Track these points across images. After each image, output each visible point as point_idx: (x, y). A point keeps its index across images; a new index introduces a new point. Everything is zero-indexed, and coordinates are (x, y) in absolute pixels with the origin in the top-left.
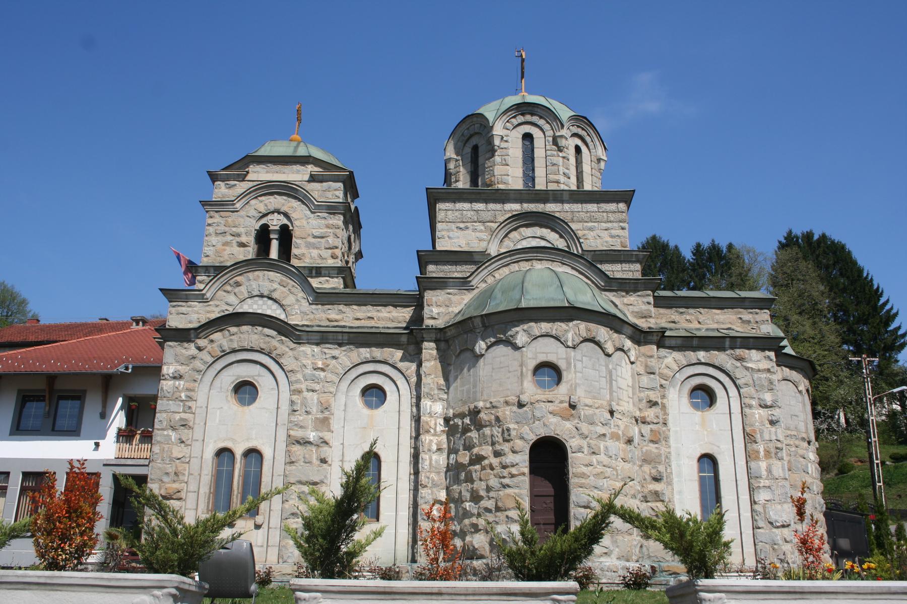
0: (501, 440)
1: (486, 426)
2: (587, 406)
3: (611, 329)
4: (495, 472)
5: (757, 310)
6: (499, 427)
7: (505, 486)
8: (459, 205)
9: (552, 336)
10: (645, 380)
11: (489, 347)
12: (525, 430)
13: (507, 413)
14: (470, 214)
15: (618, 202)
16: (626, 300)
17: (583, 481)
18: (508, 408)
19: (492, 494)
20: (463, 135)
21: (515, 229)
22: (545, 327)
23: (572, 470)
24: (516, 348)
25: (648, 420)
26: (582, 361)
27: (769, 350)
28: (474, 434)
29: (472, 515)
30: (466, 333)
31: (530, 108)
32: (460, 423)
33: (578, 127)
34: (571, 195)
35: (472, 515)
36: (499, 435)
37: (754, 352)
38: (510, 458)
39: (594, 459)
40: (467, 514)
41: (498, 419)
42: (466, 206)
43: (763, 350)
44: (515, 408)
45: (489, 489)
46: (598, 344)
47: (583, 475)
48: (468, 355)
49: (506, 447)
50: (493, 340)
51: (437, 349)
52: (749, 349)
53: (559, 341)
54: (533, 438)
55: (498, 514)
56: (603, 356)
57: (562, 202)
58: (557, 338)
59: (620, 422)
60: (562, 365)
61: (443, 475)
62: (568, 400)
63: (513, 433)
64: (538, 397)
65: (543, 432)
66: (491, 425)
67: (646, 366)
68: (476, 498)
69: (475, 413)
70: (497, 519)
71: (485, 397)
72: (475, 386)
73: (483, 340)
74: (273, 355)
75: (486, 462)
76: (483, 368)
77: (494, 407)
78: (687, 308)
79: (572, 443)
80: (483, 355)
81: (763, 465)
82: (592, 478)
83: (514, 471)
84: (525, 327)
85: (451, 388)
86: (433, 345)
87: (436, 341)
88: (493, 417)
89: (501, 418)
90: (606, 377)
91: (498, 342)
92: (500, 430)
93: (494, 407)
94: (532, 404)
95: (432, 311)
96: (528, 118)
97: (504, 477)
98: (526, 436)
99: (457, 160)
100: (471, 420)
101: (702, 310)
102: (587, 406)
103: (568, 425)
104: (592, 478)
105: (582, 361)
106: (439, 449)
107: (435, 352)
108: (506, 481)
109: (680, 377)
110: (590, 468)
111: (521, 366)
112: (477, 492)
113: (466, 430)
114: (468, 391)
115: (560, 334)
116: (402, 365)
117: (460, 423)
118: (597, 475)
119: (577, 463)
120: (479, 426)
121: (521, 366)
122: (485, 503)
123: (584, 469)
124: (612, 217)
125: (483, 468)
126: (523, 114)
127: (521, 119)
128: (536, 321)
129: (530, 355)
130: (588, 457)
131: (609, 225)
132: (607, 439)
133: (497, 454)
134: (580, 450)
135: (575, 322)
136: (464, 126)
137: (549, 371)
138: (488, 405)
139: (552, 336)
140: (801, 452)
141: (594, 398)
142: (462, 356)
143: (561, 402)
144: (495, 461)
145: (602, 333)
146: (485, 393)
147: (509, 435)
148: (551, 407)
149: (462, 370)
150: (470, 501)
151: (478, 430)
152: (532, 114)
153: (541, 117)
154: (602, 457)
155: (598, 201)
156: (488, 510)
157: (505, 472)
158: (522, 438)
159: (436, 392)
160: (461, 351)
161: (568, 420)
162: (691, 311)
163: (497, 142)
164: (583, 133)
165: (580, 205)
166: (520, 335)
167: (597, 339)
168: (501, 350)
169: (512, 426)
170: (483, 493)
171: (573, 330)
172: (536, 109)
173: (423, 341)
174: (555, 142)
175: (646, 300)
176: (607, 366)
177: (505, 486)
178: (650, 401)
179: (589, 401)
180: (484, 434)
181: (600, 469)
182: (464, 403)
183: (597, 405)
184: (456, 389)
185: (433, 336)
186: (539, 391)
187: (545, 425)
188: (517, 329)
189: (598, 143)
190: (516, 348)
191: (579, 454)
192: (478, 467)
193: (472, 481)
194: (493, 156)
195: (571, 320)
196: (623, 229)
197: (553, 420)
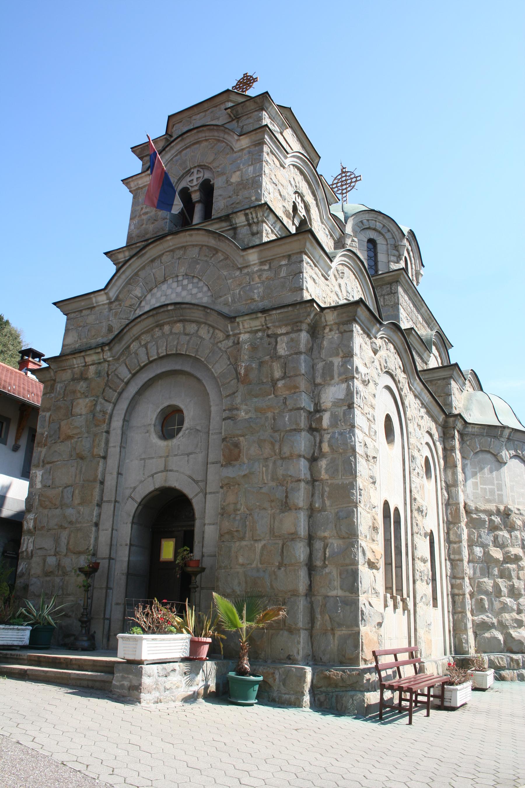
1: (517, 530)
11: (511, 458)
14: (409, 310)
20: (362, 222)
28: (504, 534)
29: (513, 610)
30: (488, 436)
32: (487, 519)
35: (513, 610)
40: (505, 608)
48: (488, 456)
68: (514, 593)
69: (506, 514)
72: (500, 488)
73: (508, 451)
74: (403, 393)
80: (506, 463)
85: (470, 482)
91: (516, 456)
93: (521, 514)
99: (353, 241)
100: (501, 519)
112: (518, 589)
113: (493, 528)
114: (492, 492)
116: (438, 444)
117: (487, 519)
120: (511, 528)
136: (367, 216)
138: (517, 512)
142: (481, 456)
149: (482, 469)
150: (509, 597)
151: (510, 532)
160: (482, 451)
180: (516, 537)
182: (489, 501)
184: (475, 485)
192: (514, 566)
193: (510, 578)
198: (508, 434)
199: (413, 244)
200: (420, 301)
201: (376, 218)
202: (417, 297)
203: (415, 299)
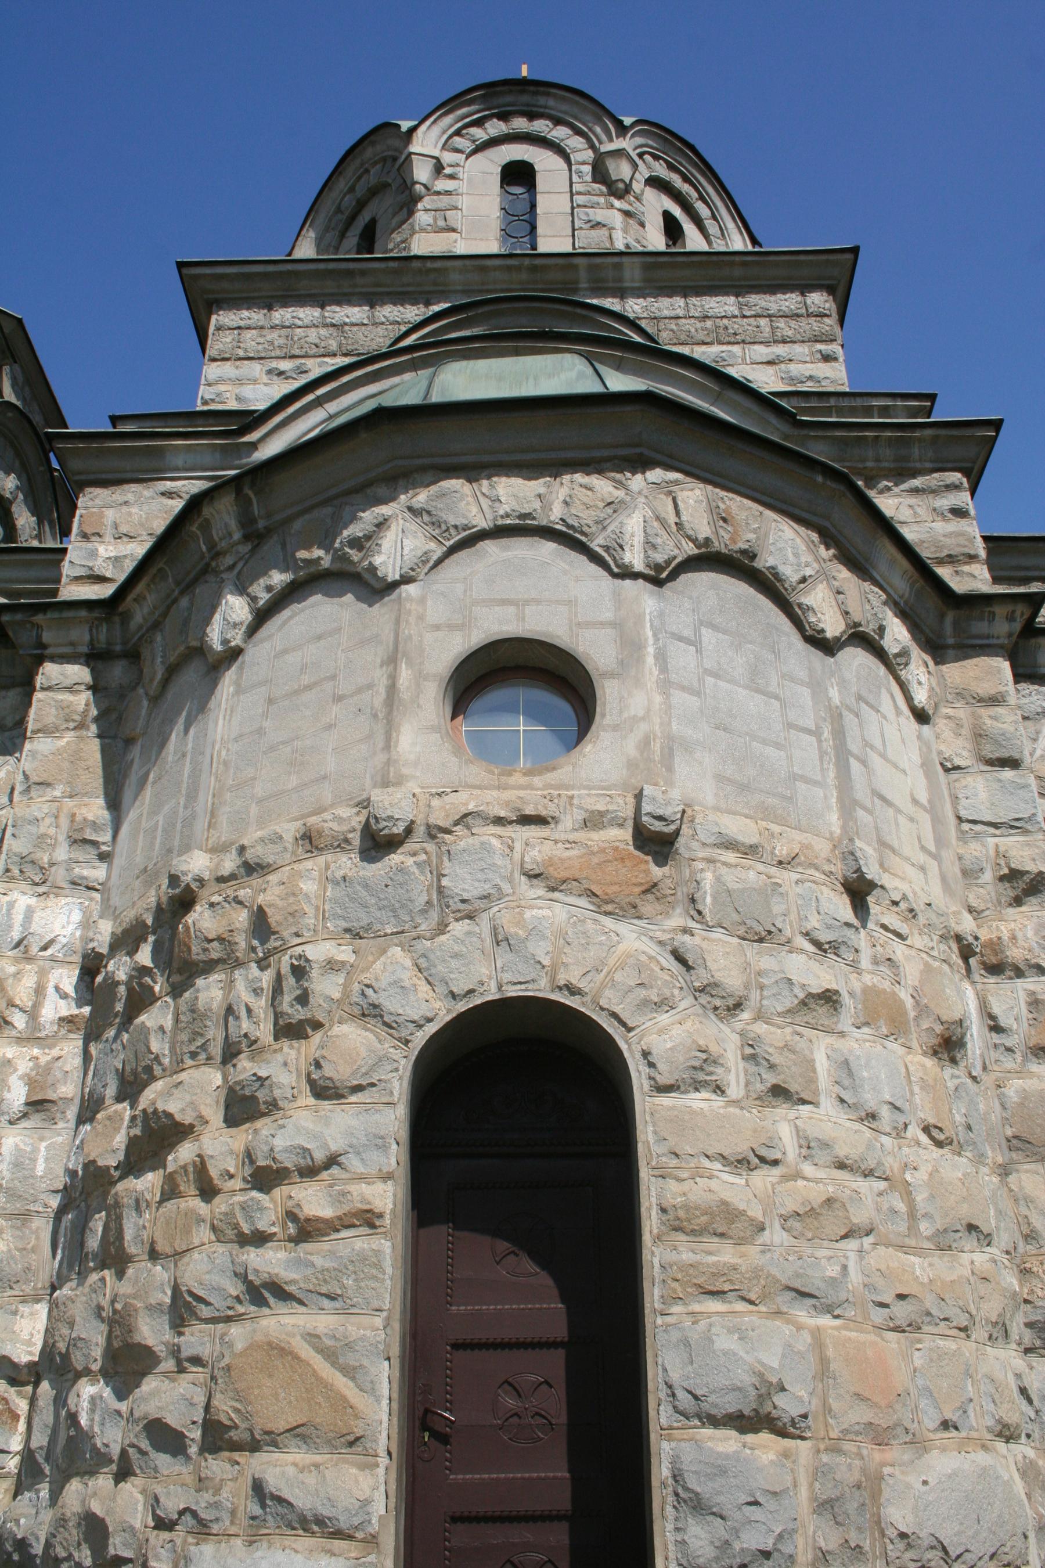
0: (264, 1032)
1: (208, 967)
2: (730, 845)
3: (828, 538)
4: (221, 1205)
6: (263, 964)
7: (263, 1292)
8: (282, 315)
9: (547, 533)
10: (981, 793)
11: (262, 616)
12: (392, 968)
13: (307, 889)
15: (804, 289)
17: (725, 1254)
18: (315, 864)
19: (196, 1339)
20: (339, 210)
22: (513, 493)
23: (655, 1194)
24: (375, 589)
25: (1015, 954)
26: (695, 642)
31: (525, 98)
34: (646, 268)
36: (260, 1005)
38: (301, 1127)
39: (783, 1126)
41: (261, 925)
42: (308, 314)
44: (348, 863)
45: (182, 1309)
46: (768, 585)
47: (723, 1223)
49: (282, 1068)
50: (278, 578)
51: (94, 688)
53: (582, 548)
54: (429, 1009)
55: (217, 1466)
58: (570, 539)
59: (899, 950)
60: (596, 651)
61: (42, 1228)
62: (630, 812)
63: (326, 987)
64: (467, 801)
65: (487, 976)
66: (230, 962)
67: (979, 736)
70: (201, 1502)
71: (224, 832)
73: (241, 590)
75: (184, 1153)
76: (232, 709)
77: (251, 869)
79: (655, 1039)
80: (234, 654)
82: (776, 1235)
83: (314, 1200)
84: (421, 497)
86: (79, 673)
87: (94, 658)
88: (242, 918)
89: (274, 918)
90: (817, 733)
92: (266, 979)
94: (433, 832)
95: (94, 554)
96: (520, 124)
97: (260, 1239)
98: (391, 1003)
102: (730, 845)
103: (632, 939)
104: (776, 1235)
105: (695, 642)
106: (37, 1105)
107: (83, 699)
108: (271, 1261)
110: (764, 1178)
111: (392, 661)
115: (583, 516)
118: (804, 1219)
119: (685, 1149)
121: (392, 661)
122: (167, 1396)
123: (729, 1186)
124: (785, 328)
125: (170, 1192)
126: (504, 117)
127: (495, 128)
128: (473, 470)
129: (436, 611)
130: (750, 1118)
131: (780, 350)
132: (845, 1021)
133: (242, 1107)
134: (701, 1075)
135: (656, 475)
137: (523, 679)
139: (547, 533)
143: (593, 821)
144: (219, 1145)
146: (223, 820)
147: (303, 999)
148: (535, 846)
152: (532, 116)
153: (558, 122)
154: (826, 1119)
155: (738, 288)
156: (164, 1437)
157: (267, 1210)
158: (371, 1013)
159: (62, 853)
161: (630, 911)
163: (422, 172)
165: (679, 301)
166: (397, 537)
167: (765, 561)
168: (322, 613)
169: (317, 952)
170: (151, 1331)
171: (651, 508)
172: (542, 100)
173: (40, 660)
174: (600, 174)
175: (947, 501)
177: (263, 1292)
178: (1013, 876)
179: (742, 828)
181: (818, 1182)
183: (782, 850)
185: (81, 635)
186: (477, 772)
187: (500, 939)
188: (384, 510)
189: (730, 225)
190: (375, 589)
191: (698, 1101)
194: (411, 213)
195: (640, 464)
196: (827, 358)
197: (549, 912)
198: (233, 524)
199: (551, 102)
200: (395, 272)
201: (362, 165)
202: (363, 273)
203: (359, 280)
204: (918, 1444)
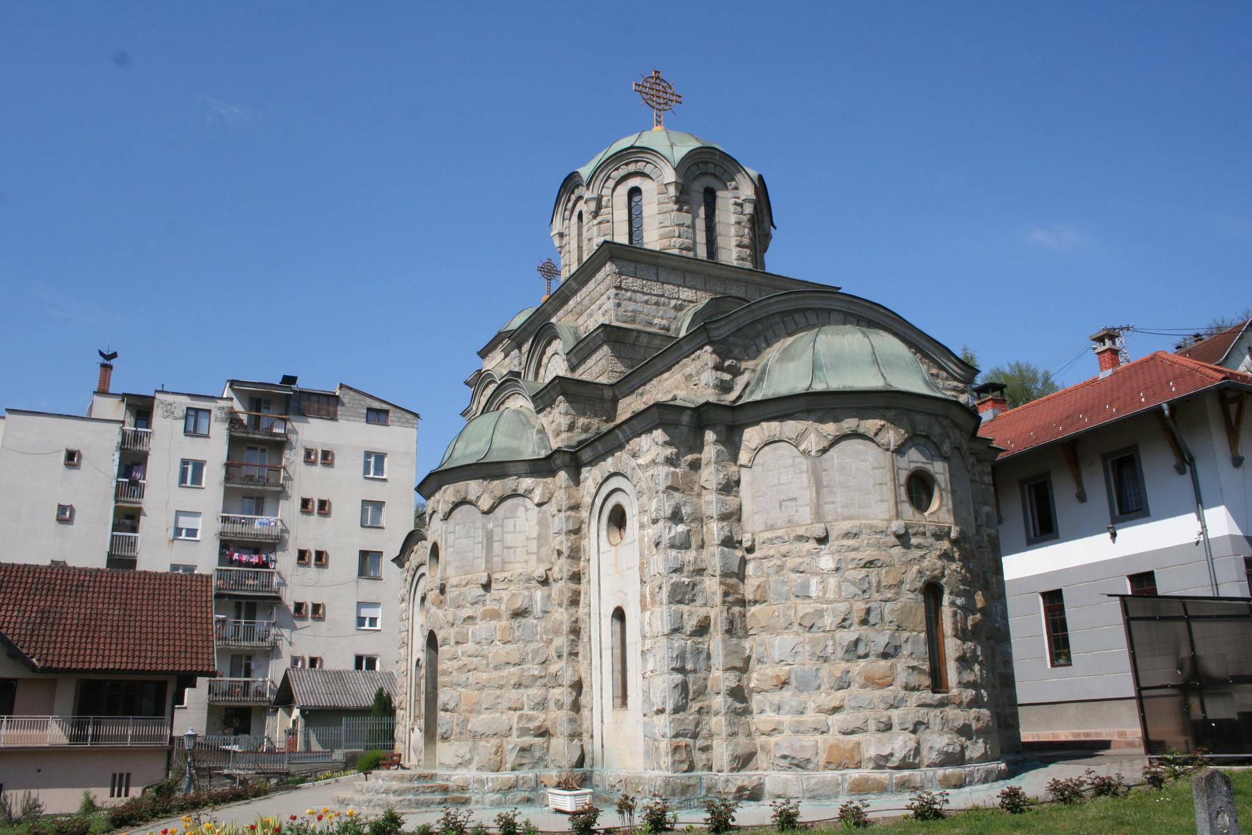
3: (484, 478)
5: (698, 352)
15: (604, 264)
16: (551, 418)
21: (543, 353)
26: (454, 532)
27: (656, 428)
33: (627, 164)
37: (643, 436)
39: (460, 649)
43: (650, 431)
46: (470, 503)
47: (445, 673)
52: (639, 435)
56: (480, 515)
57: (575, 293)
59: (503, 593)
78: (644, 384)
81: (648, 614)
82: (455, 673)
101: (655, 381)
105: (454, 532)
109: (599, 501)
118: (460, 669)
124: (603, 287)
130: (454, 649)
132: (478, 621)
140: (791, 562)
141: (467, 573)
145: (473, 488)
154: (470, 647)
162: (648, 387)
164: (632, 168)
176: (484, 526)
181: (465, 660)
189: (662, 164)
195: (440, 488)
204: (480, 713)
